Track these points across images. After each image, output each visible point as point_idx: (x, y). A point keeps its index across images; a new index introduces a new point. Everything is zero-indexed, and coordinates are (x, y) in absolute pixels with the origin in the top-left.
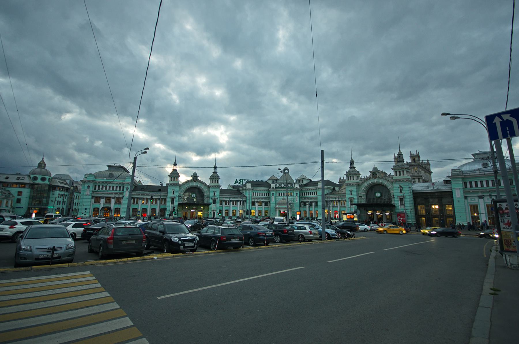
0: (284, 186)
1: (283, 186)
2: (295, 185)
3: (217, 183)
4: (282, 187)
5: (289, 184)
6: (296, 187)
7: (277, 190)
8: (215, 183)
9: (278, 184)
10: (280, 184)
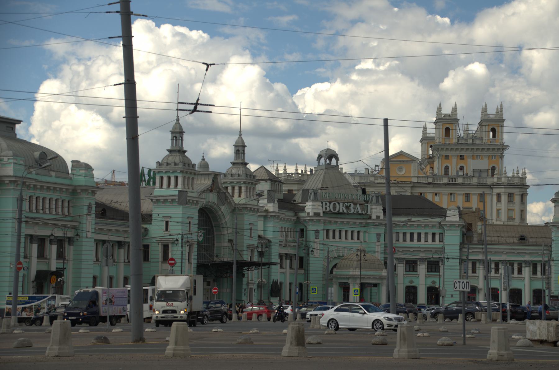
1: (341, 211)
2: (374, 210)
4: (338, 213)
5: (358, 206)
6: (378, 215)
9: (330, 203)
10: (334, 204)
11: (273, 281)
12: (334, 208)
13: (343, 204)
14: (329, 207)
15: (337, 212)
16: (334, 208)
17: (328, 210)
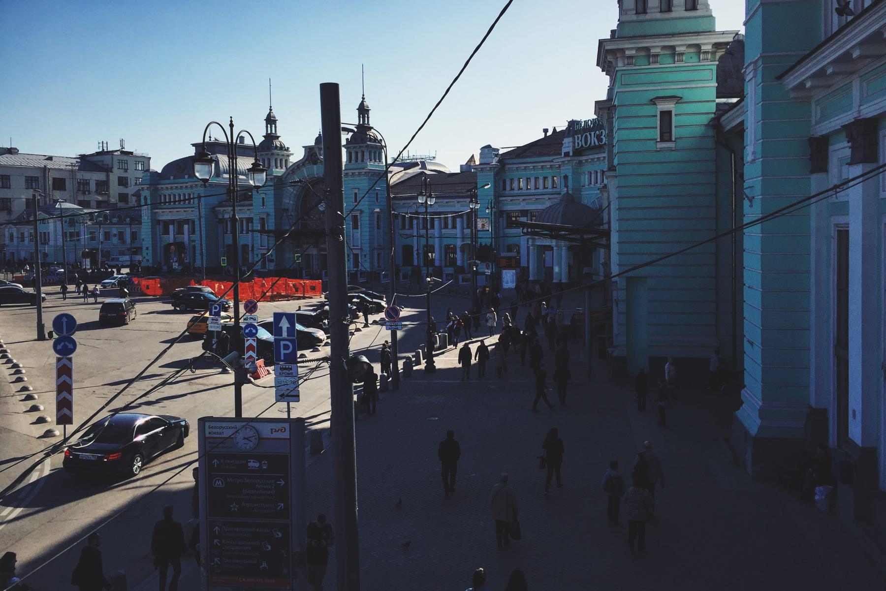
0: (597, 144)
3: (363, 161)
7: (580, 162)
8: (357, 161)
11: (481, 244)
12: (586, 143)
13: (595, 134)
14: (581, 141)
15: (589, 146)
16: (586, 143)
17: (580, 145)
